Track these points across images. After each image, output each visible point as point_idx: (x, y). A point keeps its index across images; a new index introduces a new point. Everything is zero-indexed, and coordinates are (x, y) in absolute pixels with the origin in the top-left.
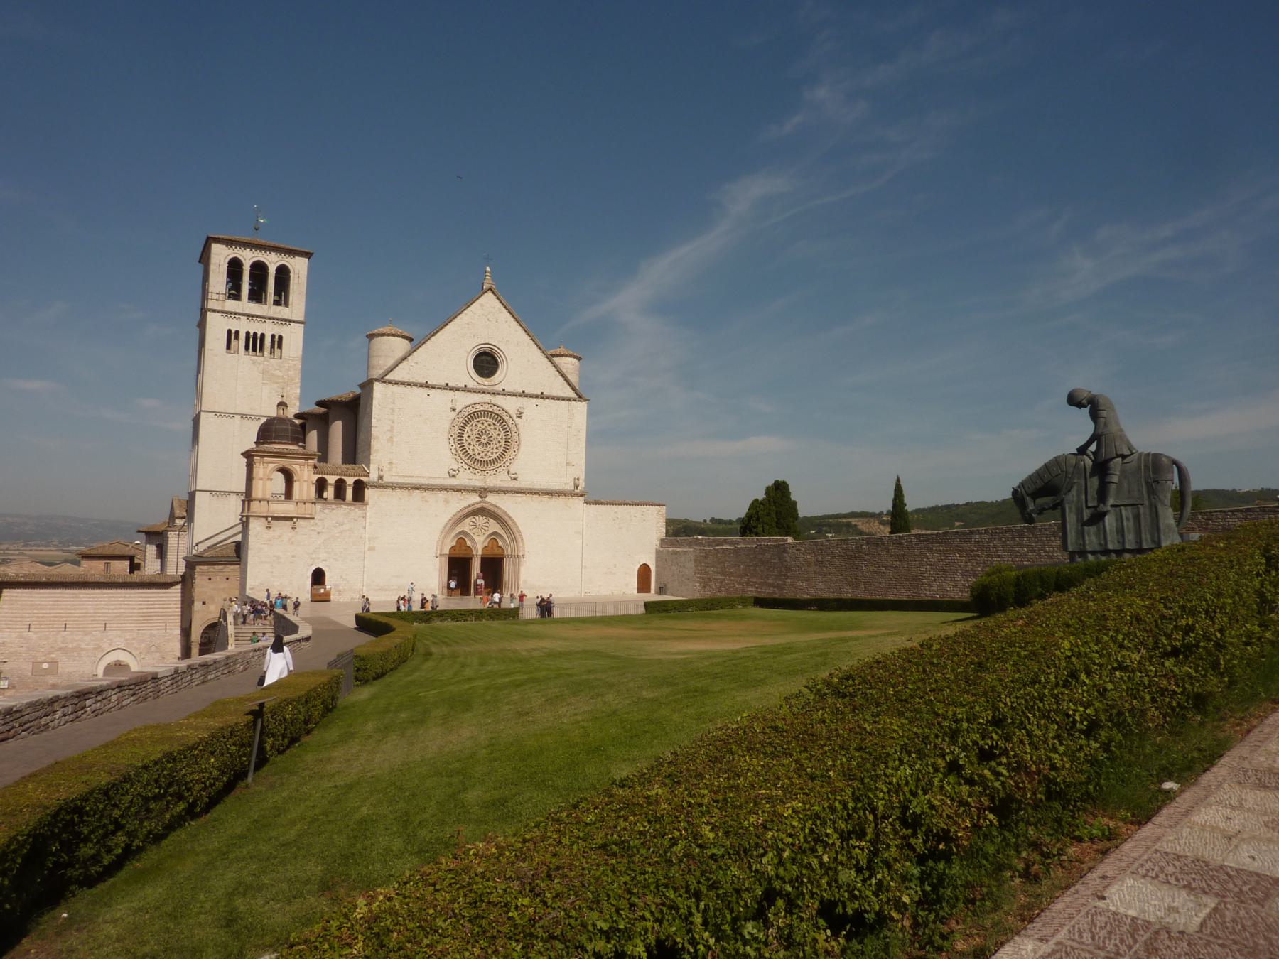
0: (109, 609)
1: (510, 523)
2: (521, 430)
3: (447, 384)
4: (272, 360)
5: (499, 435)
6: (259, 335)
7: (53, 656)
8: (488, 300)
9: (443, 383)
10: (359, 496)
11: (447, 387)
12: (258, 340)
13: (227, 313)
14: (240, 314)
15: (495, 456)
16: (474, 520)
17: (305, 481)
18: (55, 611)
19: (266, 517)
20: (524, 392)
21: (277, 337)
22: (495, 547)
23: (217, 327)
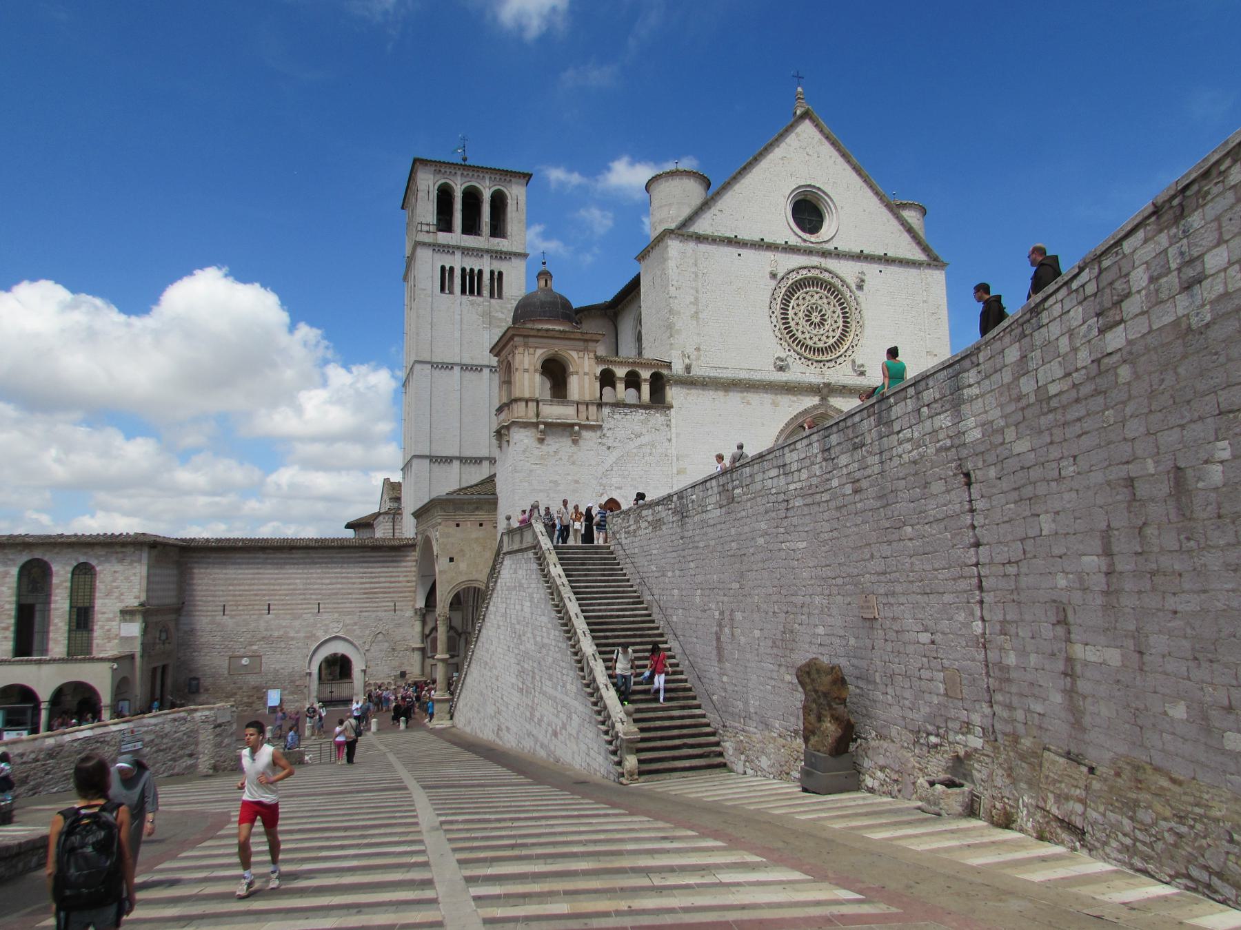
0: (322, 584)
2: (863, 306)
3: (762, 240)
4: (492, 300)
5: (834, 312)
6: (476, 272)
7: (255, 647)
8: (806, 128)
9: (757, 238)
10: (658, 400)
11: (762, 245)
12: (476, 278)
13: (439, 245)
14: (454, 247)
15: (831, 341)
17: (586, 374)
18: (256, 587)
19: (536, 425)
20: (862, 251)
21: (496, 274)
23: (428, 266)
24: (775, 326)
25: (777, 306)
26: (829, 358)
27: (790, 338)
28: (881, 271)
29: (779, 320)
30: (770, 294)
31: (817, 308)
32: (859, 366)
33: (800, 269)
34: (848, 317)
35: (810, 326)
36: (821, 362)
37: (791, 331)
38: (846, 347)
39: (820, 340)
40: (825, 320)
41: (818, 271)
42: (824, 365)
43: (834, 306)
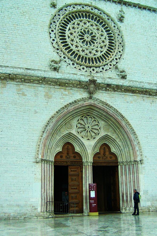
1: (123, 123)
2: (124, 33)
5: (102, 35)
15: (99, 54)
16: (82, 122)
22: (107, 153)
24: (53, 40)
25: (57, 26)
29: (57, 36)
30: (50, 18)
32: (121, 72)
36: (90, 67)
38: (111, 59)
39: (90, 53)
40: (95, 40)
42: (93, 70)
43: (102, 31)
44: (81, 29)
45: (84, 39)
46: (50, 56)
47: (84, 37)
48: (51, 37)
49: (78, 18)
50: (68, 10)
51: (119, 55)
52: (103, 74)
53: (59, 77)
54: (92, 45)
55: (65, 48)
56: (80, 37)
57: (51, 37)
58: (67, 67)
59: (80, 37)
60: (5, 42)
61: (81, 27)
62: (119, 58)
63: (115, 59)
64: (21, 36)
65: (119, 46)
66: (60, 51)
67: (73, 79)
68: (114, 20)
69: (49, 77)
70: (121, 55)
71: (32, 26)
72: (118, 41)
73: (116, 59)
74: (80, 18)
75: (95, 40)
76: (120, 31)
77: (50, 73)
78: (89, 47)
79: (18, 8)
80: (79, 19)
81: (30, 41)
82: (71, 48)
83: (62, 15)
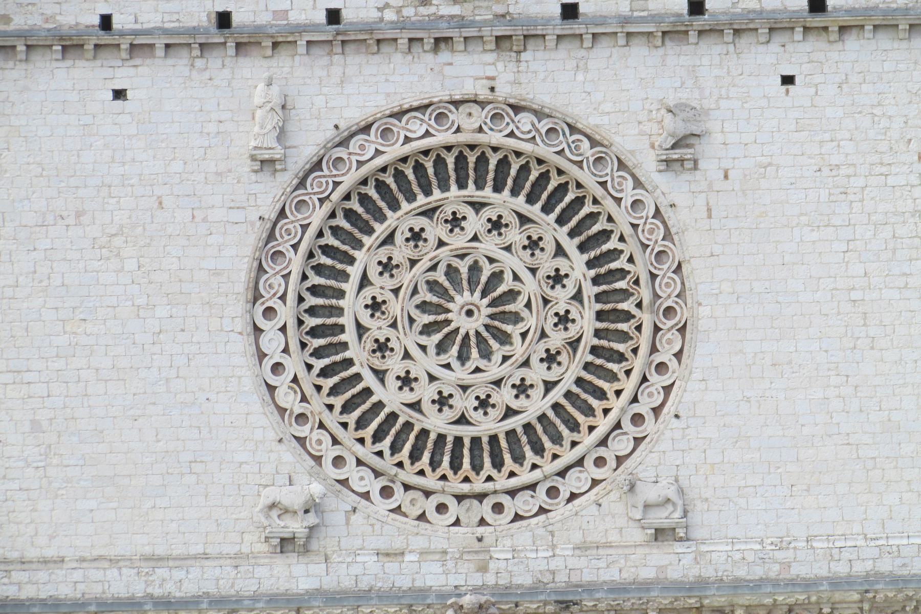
3: (224, 20)
5: (557, 279)
24: (277, 368)
26: (525, 477)
27: (347, 408)
28: (788, 80)
30: (253, 236)
31: (475, 268)
33: (398, 115)
34: (625, 294)
35: (441, 348)
36: (481, 497)
37: (358, 377)
38: (604, 425)
39: (484, 404)
40: (516, 318)
41: (480, 116)
42: (498, 508)
43: (560, 251)
44: (433, 268)
45: (448, 322)
46: (263, 471)
47: (448, 311)
48: (262, 356)
49: (411, 198)
50: (354, 158)
51: (652, 389)
52: (550, 528)
53: (306, 587)
54: (497, 358)
55: (338, 402)
56: (427, 319)
57: (262, 356)
58: (354, 518)
59: (427, 319)
60: (35, 425)
61: (432, 254)
62: (657, 411)
63: (627, 425)
64: (106, 381)
65: (657, 329)
66: (312, 429)
67: (379, 585)
68: (635, 166)
69: (260, 591)
70: (668, 389)
71: (162, 312)
72: (656, 296)
73: (638, 419)
74: (428, 192)
75: (516, 318)
76: (673, 231)
77: (261, 572)
78: (477, 370)
79: (79, 214)
80: (421, 200)
81: (154, 404)
82: (374, 399)
83: (321, 201)
